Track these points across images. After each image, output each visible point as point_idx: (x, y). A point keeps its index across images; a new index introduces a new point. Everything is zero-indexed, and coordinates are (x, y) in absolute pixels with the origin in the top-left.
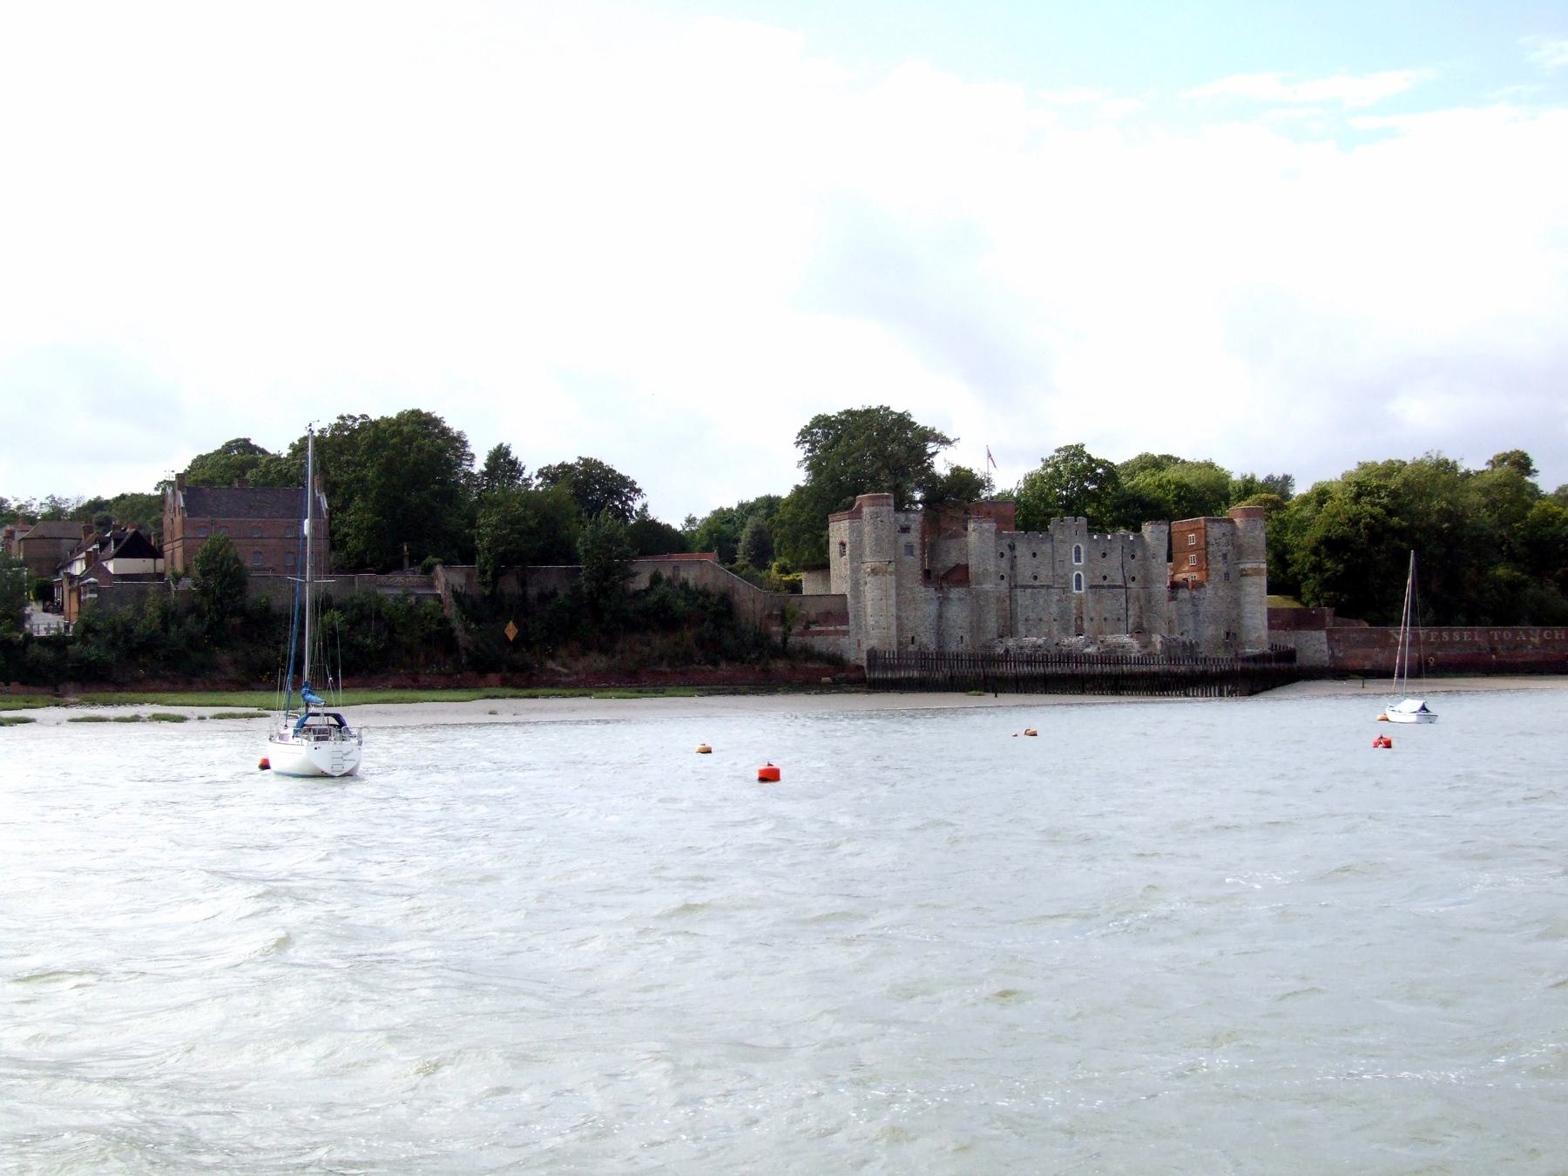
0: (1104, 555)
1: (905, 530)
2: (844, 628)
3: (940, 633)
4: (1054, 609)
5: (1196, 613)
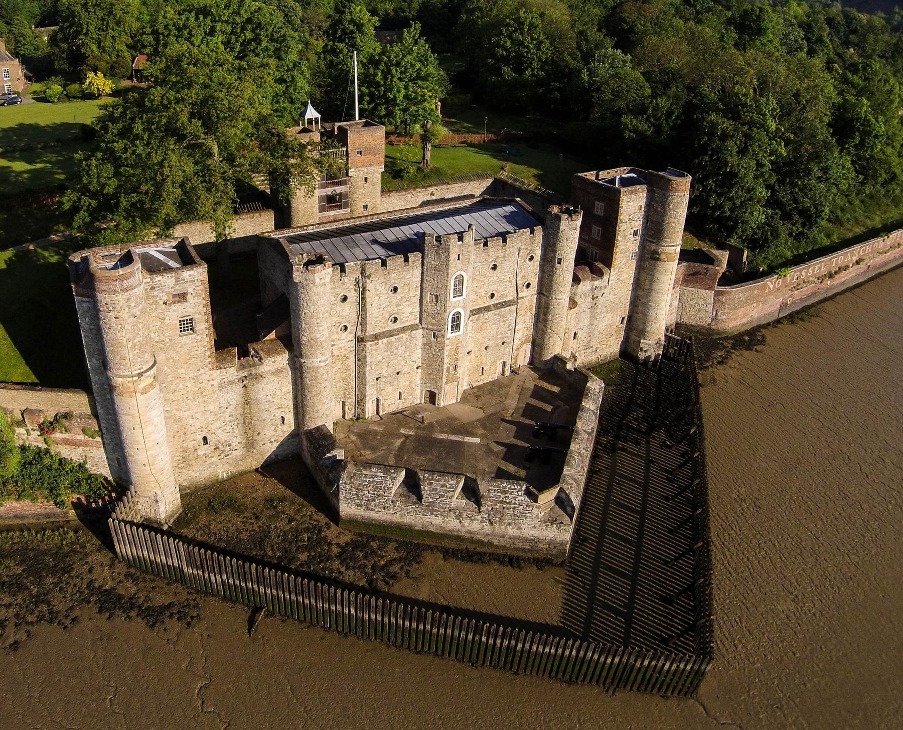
0: (495, 267)
4: (418, 355)
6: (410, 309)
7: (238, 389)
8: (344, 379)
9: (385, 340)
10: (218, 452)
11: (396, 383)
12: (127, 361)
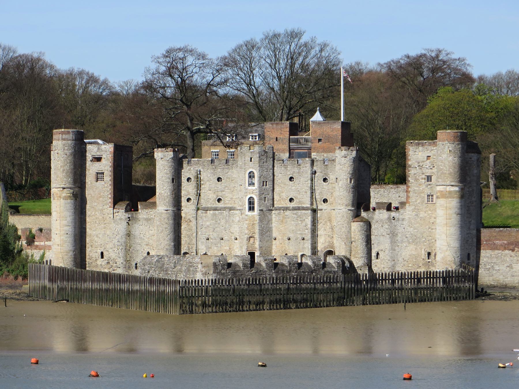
1: (98, 159)
2: (47, 243)
3: (128, 249)
5: (393, 234)
6: (231, 196)
7: (124, 224)
8: (189, 237)
9: (212, 212)
10: (109, 266)
11: (219, 245)
12: (59, 178)
